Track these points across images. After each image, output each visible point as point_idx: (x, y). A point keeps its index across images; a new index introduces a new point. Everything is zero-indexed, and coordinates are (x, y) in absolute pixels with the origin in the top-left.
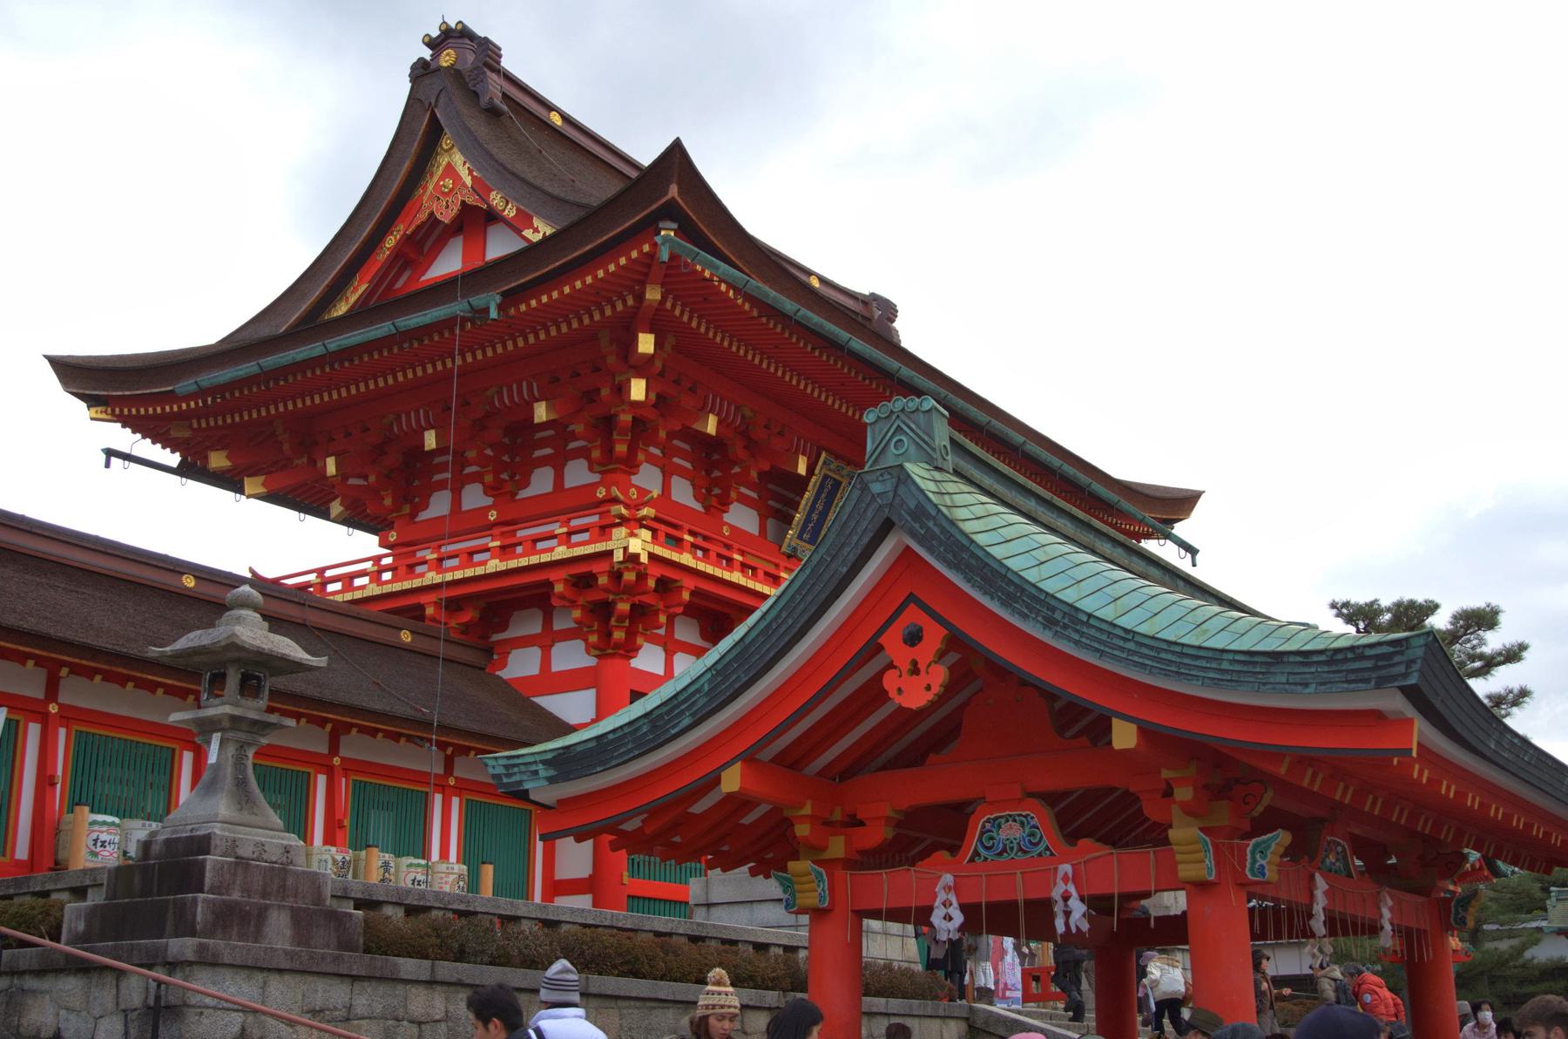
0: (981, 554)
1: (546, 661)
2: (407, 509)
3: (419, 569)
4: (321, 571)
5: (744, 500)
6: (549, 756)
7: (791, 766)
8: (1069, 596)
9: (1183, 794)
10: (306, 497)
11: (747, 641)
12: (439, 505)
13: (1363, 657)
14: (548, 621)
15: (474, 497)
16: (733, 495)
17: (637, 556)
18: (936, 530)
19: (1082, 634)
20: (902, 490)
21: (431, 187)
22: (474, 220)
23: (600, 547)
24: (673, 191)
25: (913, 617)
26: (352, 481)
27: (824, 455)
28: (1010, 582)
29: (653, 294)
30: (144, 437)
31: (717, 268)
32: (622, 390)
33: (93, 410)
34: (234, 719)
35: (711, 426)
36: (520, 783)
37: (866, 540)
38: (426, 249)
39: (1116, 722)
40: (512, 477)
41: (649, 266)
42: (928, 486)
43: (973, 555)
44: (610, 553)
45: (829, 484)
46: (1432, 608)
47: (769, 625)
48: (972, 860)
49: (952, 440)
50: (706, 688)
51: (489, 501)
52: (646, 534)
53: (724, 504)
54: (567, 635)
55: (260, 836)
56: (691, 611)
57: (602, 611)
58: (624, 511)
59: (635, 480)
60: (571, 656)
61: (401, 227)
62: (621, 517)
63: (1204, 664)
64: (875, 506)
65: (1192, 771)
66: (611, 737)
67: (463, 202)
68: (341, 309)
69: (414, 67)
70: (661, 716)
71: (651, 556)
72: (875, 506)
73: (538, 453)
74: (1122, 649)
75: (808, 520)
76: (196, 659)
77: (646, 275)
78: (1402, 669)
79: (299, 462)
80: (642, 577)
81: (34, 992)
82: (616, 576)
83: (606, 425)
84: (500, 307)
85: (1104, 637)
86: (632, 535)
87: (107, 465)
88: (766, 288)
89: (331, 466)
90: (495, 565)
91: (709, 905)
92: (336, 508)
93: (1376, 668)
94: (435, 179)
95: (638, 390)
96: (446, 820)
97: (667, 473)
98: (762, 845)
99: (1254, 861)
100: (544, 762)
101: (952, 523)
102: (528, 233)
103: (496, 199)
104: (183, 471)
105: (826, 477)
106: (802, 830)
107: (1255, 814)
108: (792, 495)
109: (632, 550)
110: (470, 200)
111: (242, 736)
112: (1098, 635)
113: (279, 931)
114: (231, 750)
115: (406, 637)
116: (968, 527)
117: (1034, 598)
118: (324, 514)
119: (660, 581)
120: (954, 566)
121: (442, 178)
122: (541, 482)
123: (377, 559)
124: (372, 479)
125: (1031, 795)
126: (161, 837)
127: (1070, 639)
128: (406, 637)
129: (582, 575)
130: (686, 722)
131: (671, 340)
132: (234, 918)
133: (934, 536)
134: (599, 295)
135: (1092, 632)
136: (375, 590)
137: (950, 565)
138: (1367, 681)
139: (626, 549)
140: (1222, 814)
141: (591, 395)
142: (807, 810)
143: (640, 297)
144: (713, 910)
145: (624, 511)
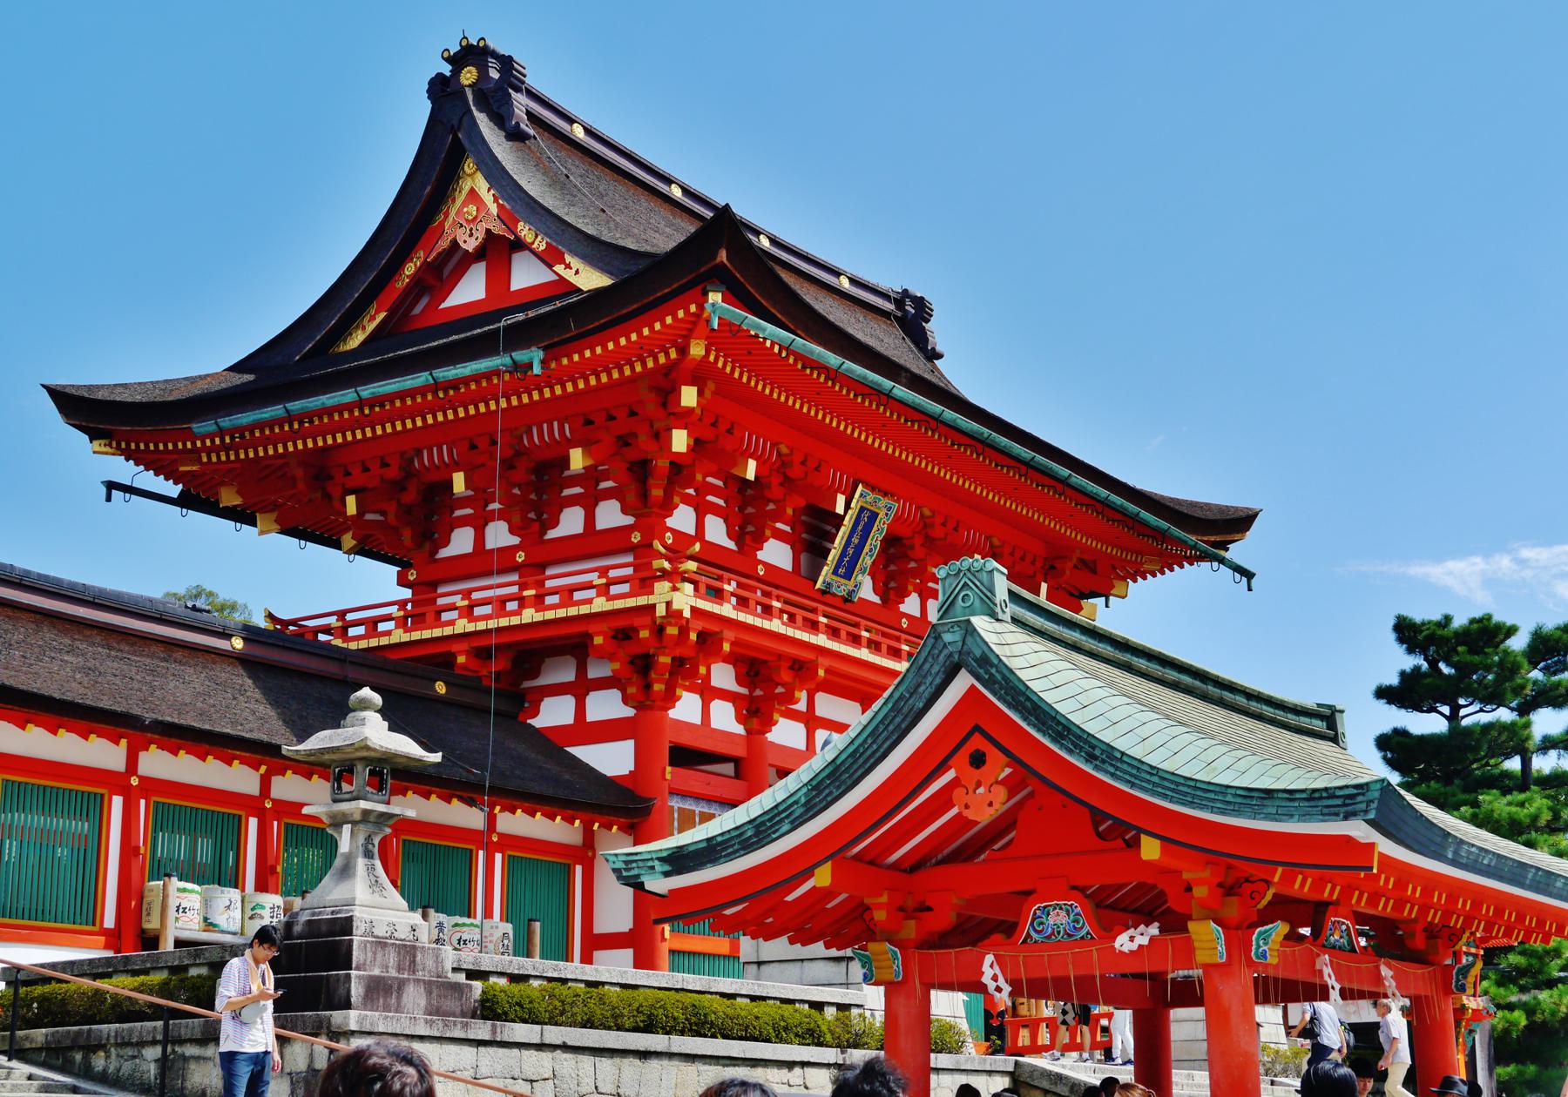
2: (427, 546)
3: (445, 616)
4: (341, 614)
5: (780, 536)
6: (665, 854)
7: (872, 863)
8: (1106, 737)
9: (1200, 892)
10: (317, 528)
12: (461, 542)
13: (1334, 797)
14: (581, 670)
15: (499, 535)
16: (768, 533)
17: (680, 612)
18: (999, 677)
19: (1117, 768)
20: (969, 640)
21: (453, 213)
22: (498, 251)
23: (642, 601)
24: (723, 256)
25: (977, 742)
26: (369, 517)
27: (860, 487)
28: (1059, 723)
29: (697, 350)
30: (147, 469)
31: (764, 330)
33: (96, 443)
34: (366, 813)
36: (638, 876)
37: (938, 681)
38: (446, 272)
39: (1145, 839)
40: (539, 516)
41: (694, 323)
43: (1028, 699)
44: (654, 606)
45: (866, 515)
46: (1511, 631)
47: (855, 751)
48: (1025, 941)
50: (803, 800)
51: (516, 540)
53: (759, 542)
55: (391, 916)
56: (727, 659)
57: (642, 665)
58: (667, 565)
59: (670, 522)
60: (606, 706)
62: (663, 570)
63: (1212, 796)
64: (946, 652)
65: (1206, 874)
67: (488, 231)
68: (356, 340)
69: (432, 82)
70: (763, 823)
71: (694, 610)
72: (946, 652)
73: (567, 492)
74: (1148, 781)
75: (844, 553)
76: (327, 757)
77: (691, 330)
78: (1363, 806)
80: (684, 631)
81: (198, 1059)
82: (659, 630)
83: (641, 471)
84: (544, 363)
86: (675, 589)
87: (109, 499)
90: (529, 615)
91: (759, 964)
92: (348, 540)
93: (1345, 805)
94: (459, 203)
95: (680, 441)
96: (491, 875)
97: (702, 510)
98: (839, 927)
99: (1259, 946)
100: (659, 859)
101: (1011, 671)
102: (559, 268)
103: (525, 231)
104: (184, 501)
105: (862, 509)
106: (880, 915)
107: (1261, 906)
108: (829, 528)
109: (675, 606)
110: (498, 229)
111: (370, 828)
113: (415, 998)
114: (361, 839)
115: (440, 688)
117: (1080, 738)
118: (337, 545)
121: (465, 204)
122: (571, 522)
123: (402, 604)
124: (392, 516)
125: (1074, 888)
126: (304, 917)
127: (1106, 772)
128: (440, 688)
129: (622, 627)
130: (786, 827)
131: (711, 386)
132: (379, 990)
133: (995, 682)
135: (1125, 767)
136: (400, 636)
137: (1009, 706)
138: (1337, 814)
139: (669, 604)
140: (1232, 908)
141: (625, 441)
142: (884, 899)
143: (683, 350)
144: (763, 967)
145: (667, 565)
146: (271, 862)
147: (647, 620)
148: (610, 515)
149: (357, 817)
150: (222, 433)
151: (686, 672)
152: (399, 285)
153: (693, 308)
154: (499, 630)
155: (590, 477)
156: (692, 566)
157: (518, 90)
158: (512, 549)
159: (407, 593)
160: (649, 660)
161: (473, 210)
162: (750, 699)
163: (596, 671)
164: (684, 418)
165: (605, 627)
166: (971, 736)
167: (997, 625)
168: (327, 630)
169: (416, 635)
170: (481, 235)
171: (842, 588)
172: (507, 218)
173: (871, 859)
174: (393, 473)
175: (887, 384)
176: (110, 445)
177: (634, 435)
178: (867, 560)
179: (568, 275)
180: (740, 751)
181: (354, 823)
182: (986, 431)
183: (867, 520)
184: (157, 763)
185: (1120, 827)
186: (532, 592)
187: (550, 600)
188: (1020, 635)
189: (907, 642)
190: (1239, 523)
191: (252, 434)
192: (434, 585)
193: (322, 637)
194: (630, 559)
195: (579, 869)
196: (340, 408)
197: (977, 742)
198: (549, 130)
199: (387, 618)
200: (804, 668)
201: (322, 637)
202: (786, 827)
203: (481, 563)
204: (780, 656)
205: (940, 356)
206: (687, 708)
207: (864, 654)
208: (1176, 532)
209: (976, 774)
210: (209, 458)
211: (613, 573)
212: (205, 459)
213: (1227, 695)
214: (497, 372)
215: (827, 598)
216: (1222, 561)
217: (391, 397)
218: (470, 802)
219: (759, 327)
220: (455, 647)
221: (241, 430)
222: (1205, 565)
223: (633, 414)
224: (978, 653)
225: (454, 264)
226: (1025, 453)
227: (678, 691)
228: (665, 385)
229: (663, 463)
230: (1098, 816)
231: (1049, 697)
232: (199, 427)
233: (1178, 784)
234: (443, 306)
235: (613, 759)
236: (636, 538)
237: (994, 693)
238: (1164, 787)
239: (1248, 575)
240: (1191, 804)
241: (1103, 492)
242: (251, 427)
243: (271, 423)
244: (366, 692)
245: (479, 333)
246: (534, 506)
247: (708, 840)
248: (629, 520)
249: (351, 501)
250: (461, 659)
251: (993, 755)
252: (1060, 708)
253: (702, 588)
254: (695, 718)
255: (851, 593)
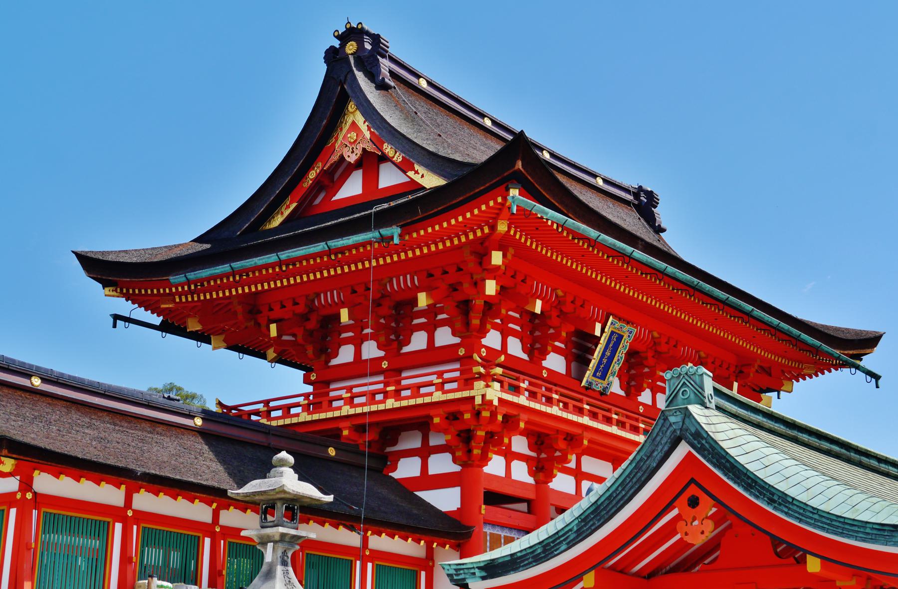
0: (732, 461)
1: (424, 467)
2: (323, 358)
3: (335, 404)
4: (266, 402)
5: (557, 350)
6: (482, 565)
7: (621, 572)
8: (781, 487)
11: (599, 503)
12: (346, 354)
14: (425, 440)
15: (371, 350)
16: (549, 348)
18: (707, 445)
19: (789, 509)
20: (687, 421)
22: (370, 162)
23: (466, 394)
24: (519, 165)
25: (693, 490)
26: (285, 338)
27: (611, 318)
28: (749, 477)
29: (502, 227)
30: (140, 306)
31: (547, 214)
32: (479, 286)
33: (107, 289)
34: (283, 535)
35: (538, 307)
36: (464, 579)
37: (666, 448)
39: (809, 558)
40: (397, 337)
42: (702, 420)
43: (728, 461)
44: (473, 398)
47: (611, 495)
49: (715, 389)
50: (575, 529)
51: (381, 354)
52: (497, 385)
53: (544, 354)
54: (439, 449)
57: (466, 437)
58: (482, 370)
59: (484, 341)
60: (441, 464)
61: (320, 164)
62: (480, 373)
63: (856, 529)
64: (671, 429)
66: (519, 554)
67: (364, 149)
69: (327, 52)
70: (548, 544)
71: (500, 400)
72: (671, 429)
73: (416, 321)
74: (811, 518)
76: (257, 498)
77: (498, 214)
79: (249, 324)
80: (494, 414)
82: (477, 414)
83: (465, 307)
84: (400, 236)
85: (801, 511)
86: (487, 386)
87: (115, 326)
88: (580, 224)
89: (273, 330)
90: (391, 403)
92: (271, 354)
95: (491, 287)
97: (505, 334)
100: (479, 568)
101: (715, 442)
102: (411, 174)
103: (388, 149)
104: (164, 328)
105: (612, 333)
108: (590, 345)
109: (488, 398)
110: (370, 148)
111: (286, 546)
112: (798, 510)
114: (279, 553)
115: (332, 452)
116: (724, 445)
117: (763, 488)
118: (264, 357)
119: (504, 416)
120: (718, 466)
121: (349, 131)
122: (418, 341)
123: (306, 396)
124: (300, 337)
127: (782, 511)
128: (332, 452)
129: (453, 412)
131: (511, 251)
133: (705, 449)
134: (466, 228)
135: (795, 508)
136: (305, 417)
137: (715, 465)
139: (483, 396)
141: (454, 288)
143: (493, 228)
145: (482, 370)
146: (219, 567)
147: (470, 407)
148: (444, 337)
149: (277, 538)
150: (189, 283)
151: (495, 442)
152: (305, 185)
153: (500, 200)
154: (371, 413)
155: (431, 311)
156: (499, 370)
157: (383, 57)
158: (380, 359)
159: (309, 389)
160: (469, 433)
161: (354, 135)
162: (538, 460)
163: (436, 440)
164: (493, 273)
165: (441, 411)
166: (688, 486)
167: (706, 412)
168: (257, 413)
169: (316, 417)
170: (359, 152)
171: (599, 385)
172: (376, 140)
173: (621, 569)
174: (301, 309)
175: (629, 249)
176: (116, 291)
177: (461, 284)
178: (616, 367)
179: (417, 178)
180: (531, 495)
181: (275, 542)
182: (696, 281)
183: (616, 340)
184: (145, 501)
185: (792, 549)
186: (393, 388)
187: (405, 393)
188: (722, 418)
189: (643, 422)
190: (870, 341)
191: (209, 283)
192: (327, 383)
193: (254, 418)
194: (457, 366)
195: (423, 574)
196: (266, 266)
197: (693, 490)
198: (405, 81)
199: (297, 405)
200: (573, 439)
201: (254, 418)
202: (563, 547)
203: (359, 369)
204: (558, 431)
205: (664, 230)
206: (495, 466)
207: (614, 430)
208: (826, 347)
209: (693, 512)
210: (181, 299)
211: (446, 376)
212: (178, 300)
213: (864, 460)
214: (370, 243)
215: (589, 392)
216: (858, 367)
217: (300, 259)
218: (351, 528)
219: (543, 212)
220: (341, 425)
221: (201, 281)
222: (846, 370)
223: (460, 270)
224: (693, 430)
225: (342, 170)
226: (722, 295)
227: (490, 455)
228: (481, 249)
229: (479, 302)
230: (776, 541)
231: (742, 460)
232: (174, 279)
233: (832, 520)
234: (334, 199)
235: (446, 500)
236: (462, 352)
237: (704, 457)
238: (823, 522)
239: (877, 377)
240: (841, 534)
241: (775, 321)
242: (208, 279)
243: (221, 276)
244: (284, 455)
245: (357, 217)
246: (396, 331)
247: (512, 555)
248: (457, 340)
249: (273, 328)
250: (346, 433)
251: (704, 499)
252: (751, 467)
253: (506, 386)
254: (503, 474)
255: (605, 389)
